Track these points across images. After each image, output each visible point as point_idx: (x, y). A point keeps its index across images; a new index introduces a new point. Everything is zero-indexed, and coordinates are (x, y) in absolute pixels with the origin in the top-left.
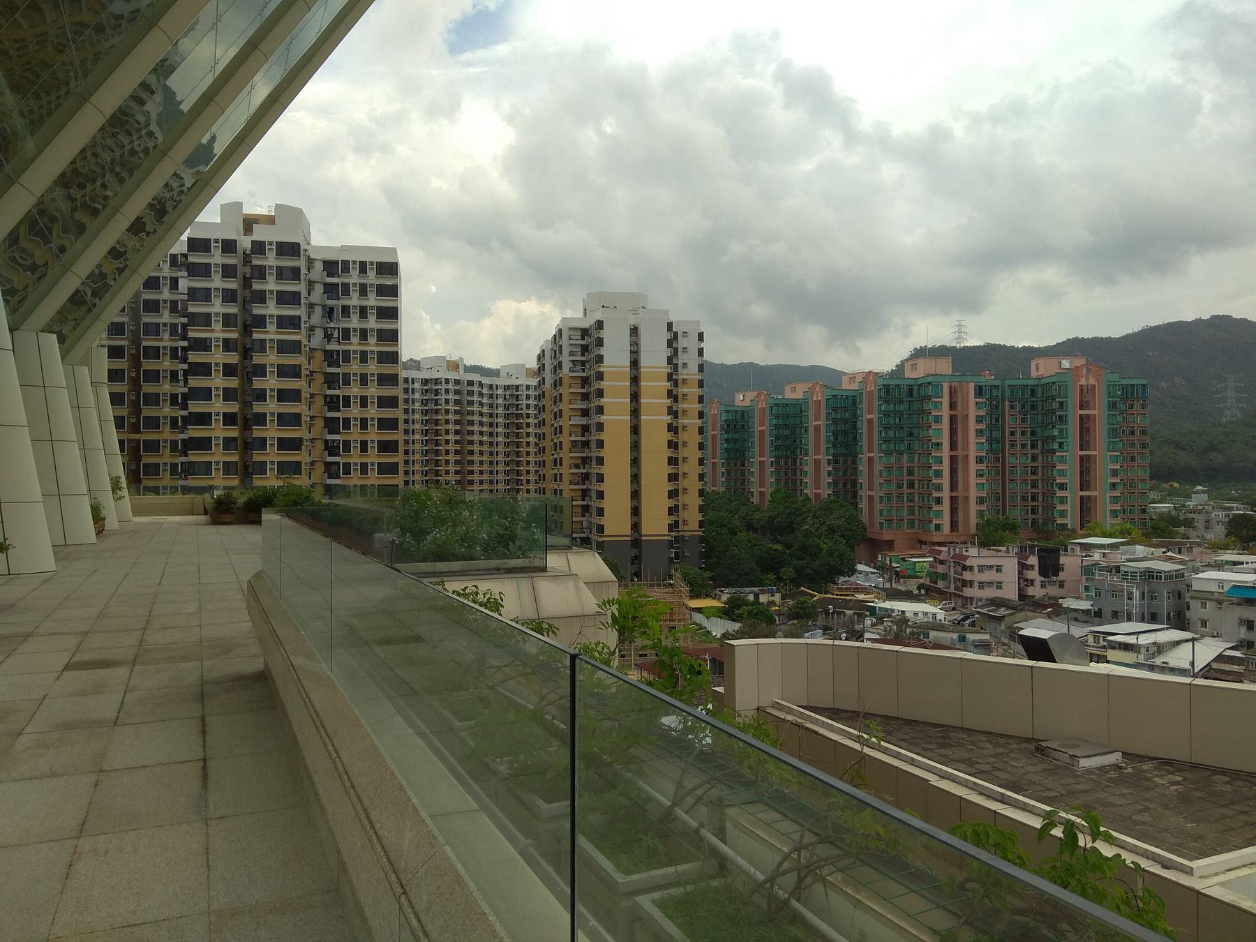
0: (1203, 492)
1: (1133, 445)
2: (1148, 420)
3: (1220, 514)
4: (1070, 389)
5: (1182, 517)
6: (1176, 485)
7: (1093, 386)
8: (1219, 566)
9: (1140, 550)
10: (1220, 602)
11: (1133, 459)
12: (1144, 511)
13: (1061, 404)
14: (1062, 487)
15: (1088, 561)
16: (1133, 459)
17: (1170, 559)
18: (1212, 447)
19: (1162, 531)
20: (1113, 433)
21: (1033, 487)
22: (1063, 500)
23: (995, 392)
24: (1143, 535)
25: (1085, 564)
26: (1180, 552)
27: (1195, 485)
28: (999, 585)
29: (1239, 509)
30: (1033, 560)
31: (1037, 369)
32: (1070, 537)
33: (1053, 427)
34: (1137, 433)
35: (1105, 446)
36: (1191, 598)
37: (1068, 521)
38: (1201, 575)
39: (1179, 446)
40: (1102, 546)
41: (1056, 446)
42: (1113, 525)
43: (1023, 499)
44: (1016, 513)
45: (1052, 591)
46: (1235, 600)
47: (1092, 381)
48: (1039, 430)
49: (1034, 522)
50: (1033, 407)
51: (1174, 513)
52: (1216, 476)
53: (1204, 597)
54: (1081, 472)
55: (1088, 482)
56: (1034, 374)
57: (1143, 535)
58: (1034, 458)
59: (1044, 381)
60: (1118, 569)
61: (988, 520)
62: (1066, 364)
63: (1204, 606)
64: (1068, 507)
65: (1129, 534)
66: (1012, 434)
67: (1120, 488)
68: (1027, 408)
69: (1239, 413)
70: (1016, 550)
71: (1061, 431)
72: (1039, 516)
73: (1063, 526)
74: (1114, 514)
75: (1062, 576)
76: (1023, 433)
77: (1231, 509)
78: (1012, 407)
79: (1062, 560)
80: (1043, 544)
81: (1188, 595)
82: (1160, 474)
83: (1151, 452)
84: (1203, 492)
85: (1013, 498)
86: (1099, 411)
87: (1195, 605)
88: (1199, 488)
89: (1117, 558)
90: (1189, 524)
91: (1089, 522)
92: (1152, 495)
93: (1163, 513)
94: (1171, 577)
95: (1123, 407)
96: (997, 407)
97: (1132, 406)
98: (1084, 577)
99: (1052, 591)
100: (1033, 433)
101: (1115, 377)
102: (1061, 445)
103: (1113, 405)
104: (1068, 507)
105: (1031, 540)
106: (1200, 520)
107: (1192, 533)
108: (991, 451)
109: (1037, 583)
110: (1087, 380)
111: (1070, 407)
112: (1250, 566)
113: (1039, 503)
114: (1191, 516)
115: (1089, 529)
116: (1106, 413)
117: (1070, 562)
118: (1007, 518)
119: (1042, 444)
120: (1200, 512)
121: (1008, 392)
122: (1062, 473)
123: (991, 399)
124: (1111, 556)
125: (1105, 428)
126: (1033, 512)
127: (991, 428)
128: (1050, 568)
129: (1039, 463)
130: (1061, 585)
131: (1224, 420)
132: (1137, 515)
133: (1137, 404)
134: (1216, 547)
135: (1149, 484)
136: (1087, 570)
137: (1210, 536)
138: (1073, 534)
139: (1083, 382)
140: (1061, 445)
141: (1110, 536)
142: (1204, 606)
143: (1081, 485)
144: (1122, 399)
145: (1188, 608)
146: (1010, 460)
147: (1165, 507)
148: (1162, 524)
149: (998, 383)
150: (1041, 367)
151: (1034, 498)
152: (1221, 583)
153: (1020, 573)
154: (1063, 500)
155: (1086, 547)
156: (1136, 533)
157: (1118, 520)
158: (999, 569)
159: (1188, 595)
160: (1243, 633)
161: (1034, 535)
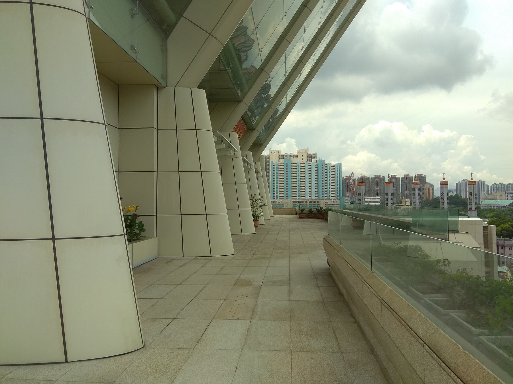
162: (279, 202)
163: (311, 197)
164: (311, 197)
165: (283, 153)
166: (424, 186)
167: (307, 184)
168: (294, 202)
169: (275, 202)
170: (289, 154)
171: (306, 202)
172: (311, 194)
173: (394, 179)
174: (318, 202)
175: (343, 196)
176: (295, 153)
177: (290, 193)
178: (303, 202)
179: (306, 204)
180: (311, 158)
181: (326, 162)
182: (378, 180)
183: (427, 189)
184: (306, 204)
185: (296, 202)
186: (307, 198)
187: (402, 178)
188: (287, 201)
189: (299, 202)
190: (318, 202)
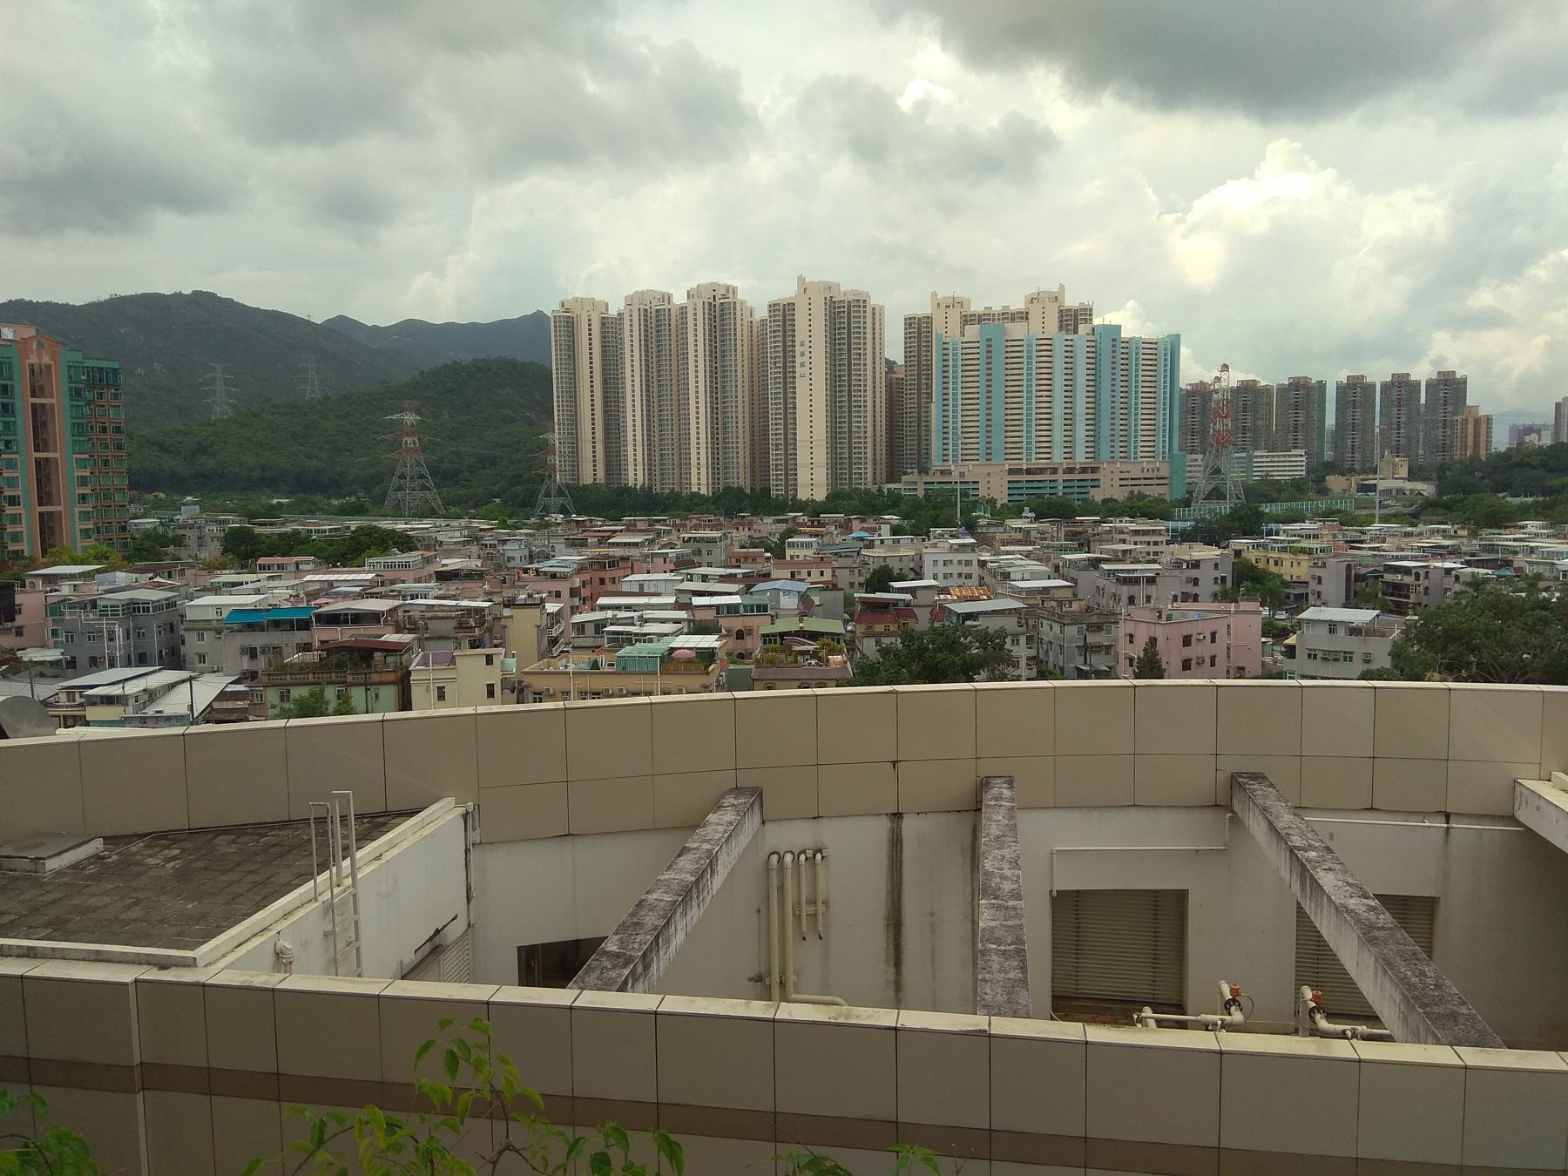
0: (194, 503)
1: (106, 446)
5: (171, 535)
6: (162, 495)
7: (48, 367)
8: (216, 589)
9: (122, 577)
11: (106, 463)
12: (124, 529)
14: (13, 501)
15: (54, 597)
16: (106, 463)
17: (159, 586)
18: (201, 449)
19: (147, 553)
20: (79, 429)
22: (15, 519)
24: (124, 558)
26: (170, 577)
27: (185, 495)
29: (235, 522)
37: (24, 547)
39: (161, 447)
40: (72, 577)
42: (85, 548)
47: (46, 360)
51: (161, 530)
52: (208, 483)
53: (201, 628)
54: (39, 481)
55: (49, 494)
57: (124, 558)
60: (94, 604)
64: (23, 528)
65: (107, 558)
73: (18, 555)
74: (86, 533)
75: (20, 620)
77: (226, 522)
79: (19, 599)
82: (142, 483)
83: (129, 455)
84: (194, 503)
86: (58, 400)
87: (191, 638)
89: (93, 589)
90: (179, 542)
91: (53, 546)
92: (133, 509)
95: (89, 396)
98: (50, 619)
101: (78, 356)
103: (76, 394)
104: (23, 528)
106: (191, 536)
107: (183, 553)
110: (39, 357)
111: (17, 392)
114: (182, 532)
115: (54, 555)
116: (67, 402)
130: (19, 632)
133: (108, 393)
134: (211, 567)
136: (54, 609)
138: (32, 563)
139: (33, 359)
143: (40, 498)
147: (149, 522)
148: (147, 544)
152: (219, 608)
154: (15, 519)
156: (116, 557)
157: (91, 542)
160: (246, 663)
162: (962, 475)
163: (1069, 454)
164: (1069, 454)
165: (977, 307)
166: (1457, 413)
167: (1059, 409)
168: (1011, 471)
169: (950, 472)
170: (997, 308)
171: (1055, 471)
172: (1070, 444)
173: (1355, 392)
174: (1094, 470)
175: (1181, 450)
176: (1018, 305)
177: (998, 441)
178: (1041, 471)
179: (1053, 477)
180: (1072, 319)
181: (1124, 335)
182: (1302, 394)
183: (1471, 420)
184: (1053, 477)
185: (1019, 471)
186: (1058, 457)
187: (1386, 387)
188: (986, 470)
189: (1029, 472)
190: (1094, 470)
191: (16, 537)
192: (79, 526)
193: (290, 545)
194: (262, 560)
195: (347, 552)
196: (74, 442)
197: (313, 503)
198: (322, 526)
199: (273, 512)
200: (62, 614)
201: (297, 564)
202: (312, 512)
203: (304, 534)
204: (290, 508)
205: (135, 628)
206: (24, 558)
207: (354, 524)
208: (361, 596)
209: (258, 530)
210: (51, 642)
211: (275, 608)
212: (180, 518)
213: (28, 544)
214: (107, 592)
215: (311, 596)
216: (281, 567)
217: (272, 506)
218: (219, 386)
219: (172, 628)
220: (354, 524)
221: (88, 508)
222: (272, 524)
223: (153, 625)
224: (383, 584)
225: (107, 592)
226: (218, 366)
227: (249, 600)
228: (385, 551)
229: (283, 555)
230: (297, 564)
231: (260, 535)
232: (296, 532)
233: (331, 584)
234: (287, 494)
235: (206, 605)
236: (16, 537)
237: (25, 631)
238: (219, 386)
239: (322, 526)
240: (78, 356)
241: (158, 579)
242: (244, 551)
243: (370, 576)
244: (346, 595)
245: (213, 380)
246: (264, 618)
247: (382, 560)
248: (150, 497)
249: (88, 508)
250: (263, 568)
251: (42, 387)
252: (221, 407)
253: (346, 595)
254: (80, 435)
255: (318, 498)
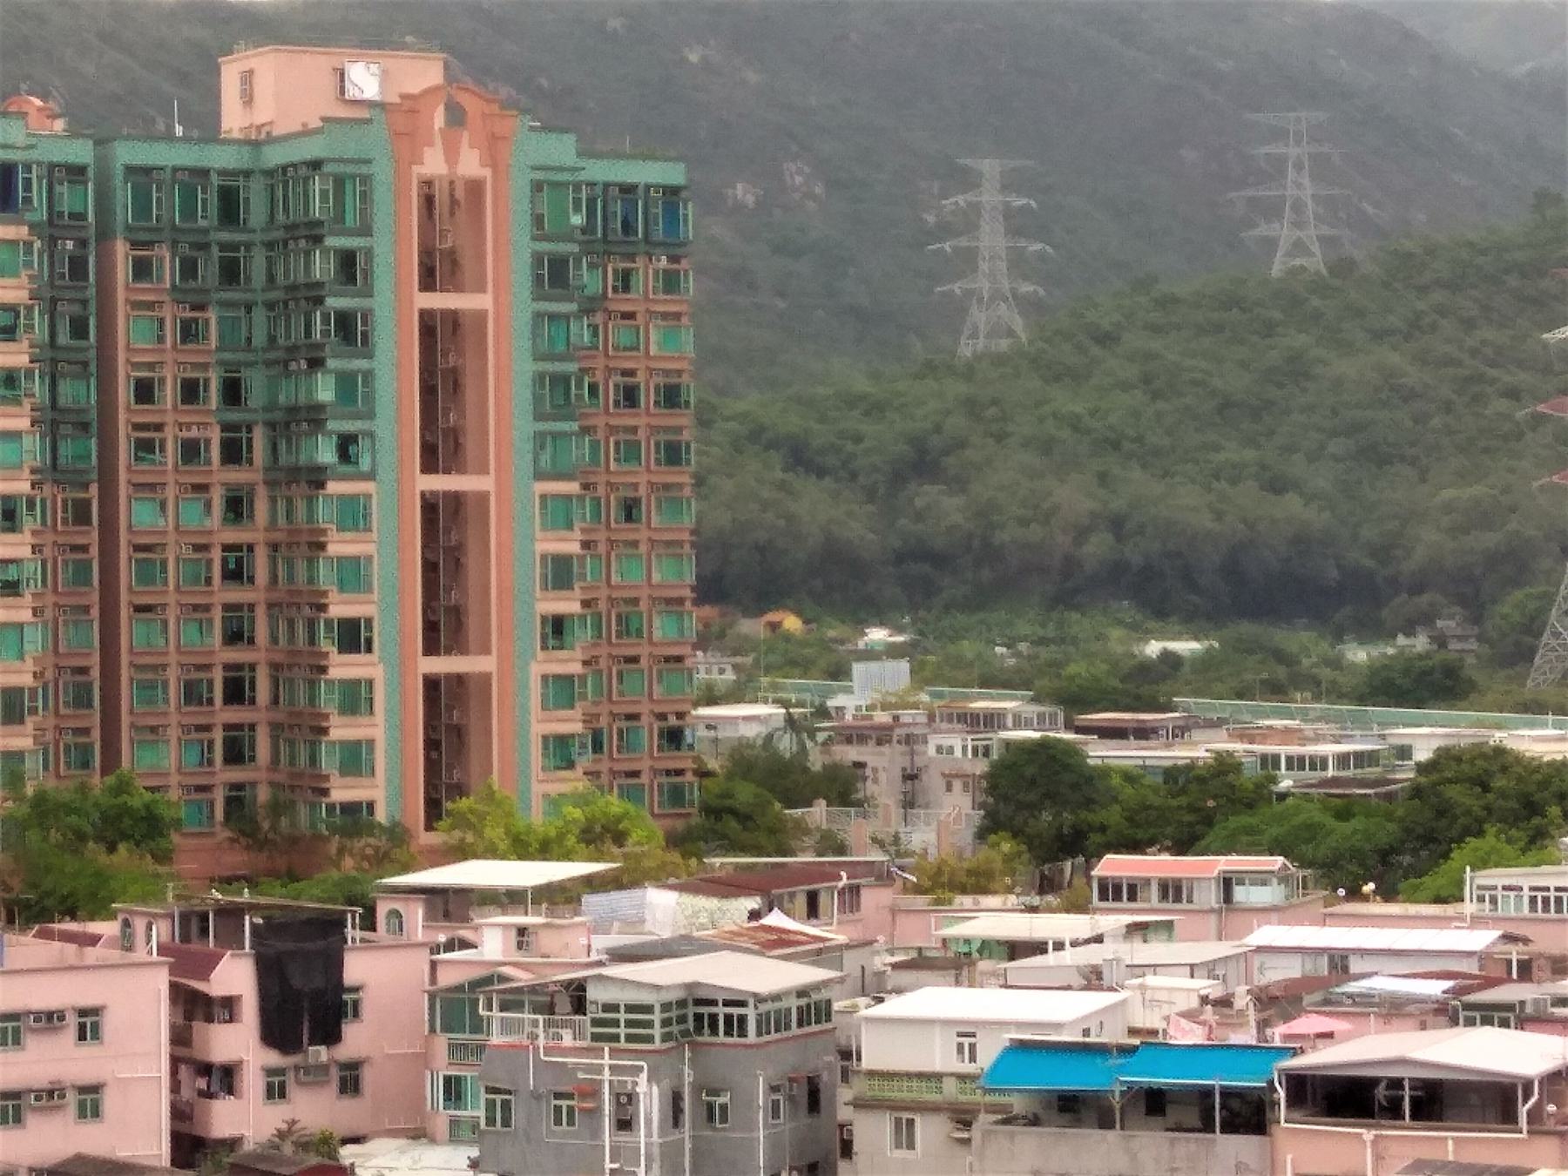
0: (893, 652)
1: (630, 452)
2: (687, 341)
3: (957, 741)
4: (382, 196)
5: (816, 761)
6: (792, 623)
7: (475, 188)
8: (958, 963)
9: (663, 908)
10: (963, 1118)
11: (630, 510)
12: (674, 737)
13: (348, 263)
14: (353, 636)
15: (457, 969)
16: (630, 510)
17: (777, 942)
18: (923, 462)
19: (742, 821)
20: (556, 394)
21: (235, 636)
22: (356, 698)
23: (67, 198)
24: (675, 841)
25: (447, 978)
26: (813, 911)
27: (861, 624)
28: (90, 1101)
29: (1023, 721)
30: (235, 976)
31: (248, 99)
32: (385, 861)
33: (316, 363)
34: (647, 398)
35: (524, 463)
36: (859, 1104)
38: (893, 1007)
39: (800, 457)
40: (512, 898)
41: (326, 454)
42: (554, 803)
43: (193, 694)
44: (161, 764)
45: (314, 1109)
46: (1018, 1104)
47: (471, 164)
48: (256, 385)
49: (237, 801)
50: (231, 272)
51: (786, 744)
52: (937, 582)
53: (905, 1100)
54: (430, 568)
55: (457, 613)
56: (233, 119)
57: (675, 841)
58: (237, 507)
59: (275, 157)
60: (577, 995)
61: (40, 799)
62: (365, 80)
63: (905, 1135)
64: (375, 728)
65: (619, 838)
66: (145, 392)
67: (582, 636)
68: (209, 271)
69: (1018, 324)
70: (162, 931)
71: (346, 383)
72: (258, 774)
73: (355, 816)
74: (560, 750)
75: (356, 1039)
76: (191, 391)
77: (992, 720)
78: (142, 269)
79: (357, 967)
80: (275, 897)
81: (845, 1094)
82: (736, 580)
83: (699, 481)
84: (893, 652)
85: (150, 688)
88: (877, 635)
89: (573, 945)
90: (842, 788)
91: (460, 790)
92: (711, 669)
93: (743, 745)
94: (782, 1021)
95: (589, 280)
96: (78, 267)
97: (625, 281)
98: (442, 1041)
99: (314, 1109)
100: (233, 392)
102: (346, 445)
103: (553, 275)
104: (375, 728)
105: (227, 882)
106: (883, 764)
107: (857, 830)
108: (53, 471)
109: (252, 1082)
110: (451, 155)
112: (1069, 956)
113: (258, 714)
114: (851, 753)
115: (462, 822)
117: (385, 975)
118: (122, 788)
119: (272, 442)
120: (882, 736)
121: (123, 196)
122: (354, 573)
123: (53, 228)
124: (547, 941)
125: (524, 368)
126: (236, 753)
127: (53, 363)
128: (306, 1008)
129: (254, 533)
130: (350, 1080)
131: (966, 350)
132: (647, 755)
133: (647, 272)
134: (949, 882)
135: (694, 618)
136: (456, 1009)
137: (921, 837)
138: (395, 849)
139: (433, 164)
140: (346, 445)
141: (545, 850)
142: (905, 1135)
143: (431, 628)
144: (588, 248)
145: (847, 1149)
146: (137, 516)
147: (751, 718)
148: (745, 793)
149: (80, 152)
150: (264, 86)
151: (237, 692)
152: (967, 1034)
153: (180, 1038)
154: (356, 698)
155: (451, 905)
156: (647, 833)
157: (573, 782)
158: (89, 1024)
159: (845, 1094)
161: (237, 860)
191: (356, 759)
192: (542, 724)
193: (1202, 811)
194: (1113, 865)
195: (1398, 843)
196: (540, 440)
197: (1281, 657)
198: (1308, 742)
199: (1146, 687)
200: (478, 1025)
201: (1227, 883)
202: (1276, 690)
203: (1252, 771)
204: (1204, 676)
205: (697, 1089)
206: (371, 828)
207: (1425, 735)
208: (1448, 1013)
209: (1099, 752)
210: (442, 1117)
211: (1147, 1042)
212: (848, 702)
213: (387, 787)
214: (622, 956)
215: (1277, 1002)
216: (1172, 890)
217: (1145, 670)
218: (992, 239)
219: (814, 1098)
220: (1425, 735)
221: (569, 663)
222: (1143, 733)
223: (756, 1083)
224: (1526, 971)
225: (622, 956)
226: (989, 167)
227: (1064, 1011)
228: (1534, 841)
229: (1182, 847)
230: (1227, 883)
231: (1105, 772)
232: (1225, 765)
233: (1339, 962)
234: (1192, 622)
235: (921, 1024)
236: (356, 759)
237: (368, 1076)
238: (992, 239)
239: (1308, 742)
240: (561, 150)
241: (776, 919)
242: (1050, 825)
243: (1482, 939)
244: (1394, 1009)
245: (969, 221)
246: (1112, 1079)
247: (1526, 877)
248: (752, 627)
249: (569, 663)
250: (1112, 891)
251: (452, 258)
252: (993, 315)
253: (1394, 1009)
254: (564, 409)
255: (1302, 642)
